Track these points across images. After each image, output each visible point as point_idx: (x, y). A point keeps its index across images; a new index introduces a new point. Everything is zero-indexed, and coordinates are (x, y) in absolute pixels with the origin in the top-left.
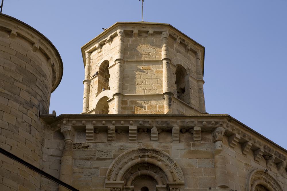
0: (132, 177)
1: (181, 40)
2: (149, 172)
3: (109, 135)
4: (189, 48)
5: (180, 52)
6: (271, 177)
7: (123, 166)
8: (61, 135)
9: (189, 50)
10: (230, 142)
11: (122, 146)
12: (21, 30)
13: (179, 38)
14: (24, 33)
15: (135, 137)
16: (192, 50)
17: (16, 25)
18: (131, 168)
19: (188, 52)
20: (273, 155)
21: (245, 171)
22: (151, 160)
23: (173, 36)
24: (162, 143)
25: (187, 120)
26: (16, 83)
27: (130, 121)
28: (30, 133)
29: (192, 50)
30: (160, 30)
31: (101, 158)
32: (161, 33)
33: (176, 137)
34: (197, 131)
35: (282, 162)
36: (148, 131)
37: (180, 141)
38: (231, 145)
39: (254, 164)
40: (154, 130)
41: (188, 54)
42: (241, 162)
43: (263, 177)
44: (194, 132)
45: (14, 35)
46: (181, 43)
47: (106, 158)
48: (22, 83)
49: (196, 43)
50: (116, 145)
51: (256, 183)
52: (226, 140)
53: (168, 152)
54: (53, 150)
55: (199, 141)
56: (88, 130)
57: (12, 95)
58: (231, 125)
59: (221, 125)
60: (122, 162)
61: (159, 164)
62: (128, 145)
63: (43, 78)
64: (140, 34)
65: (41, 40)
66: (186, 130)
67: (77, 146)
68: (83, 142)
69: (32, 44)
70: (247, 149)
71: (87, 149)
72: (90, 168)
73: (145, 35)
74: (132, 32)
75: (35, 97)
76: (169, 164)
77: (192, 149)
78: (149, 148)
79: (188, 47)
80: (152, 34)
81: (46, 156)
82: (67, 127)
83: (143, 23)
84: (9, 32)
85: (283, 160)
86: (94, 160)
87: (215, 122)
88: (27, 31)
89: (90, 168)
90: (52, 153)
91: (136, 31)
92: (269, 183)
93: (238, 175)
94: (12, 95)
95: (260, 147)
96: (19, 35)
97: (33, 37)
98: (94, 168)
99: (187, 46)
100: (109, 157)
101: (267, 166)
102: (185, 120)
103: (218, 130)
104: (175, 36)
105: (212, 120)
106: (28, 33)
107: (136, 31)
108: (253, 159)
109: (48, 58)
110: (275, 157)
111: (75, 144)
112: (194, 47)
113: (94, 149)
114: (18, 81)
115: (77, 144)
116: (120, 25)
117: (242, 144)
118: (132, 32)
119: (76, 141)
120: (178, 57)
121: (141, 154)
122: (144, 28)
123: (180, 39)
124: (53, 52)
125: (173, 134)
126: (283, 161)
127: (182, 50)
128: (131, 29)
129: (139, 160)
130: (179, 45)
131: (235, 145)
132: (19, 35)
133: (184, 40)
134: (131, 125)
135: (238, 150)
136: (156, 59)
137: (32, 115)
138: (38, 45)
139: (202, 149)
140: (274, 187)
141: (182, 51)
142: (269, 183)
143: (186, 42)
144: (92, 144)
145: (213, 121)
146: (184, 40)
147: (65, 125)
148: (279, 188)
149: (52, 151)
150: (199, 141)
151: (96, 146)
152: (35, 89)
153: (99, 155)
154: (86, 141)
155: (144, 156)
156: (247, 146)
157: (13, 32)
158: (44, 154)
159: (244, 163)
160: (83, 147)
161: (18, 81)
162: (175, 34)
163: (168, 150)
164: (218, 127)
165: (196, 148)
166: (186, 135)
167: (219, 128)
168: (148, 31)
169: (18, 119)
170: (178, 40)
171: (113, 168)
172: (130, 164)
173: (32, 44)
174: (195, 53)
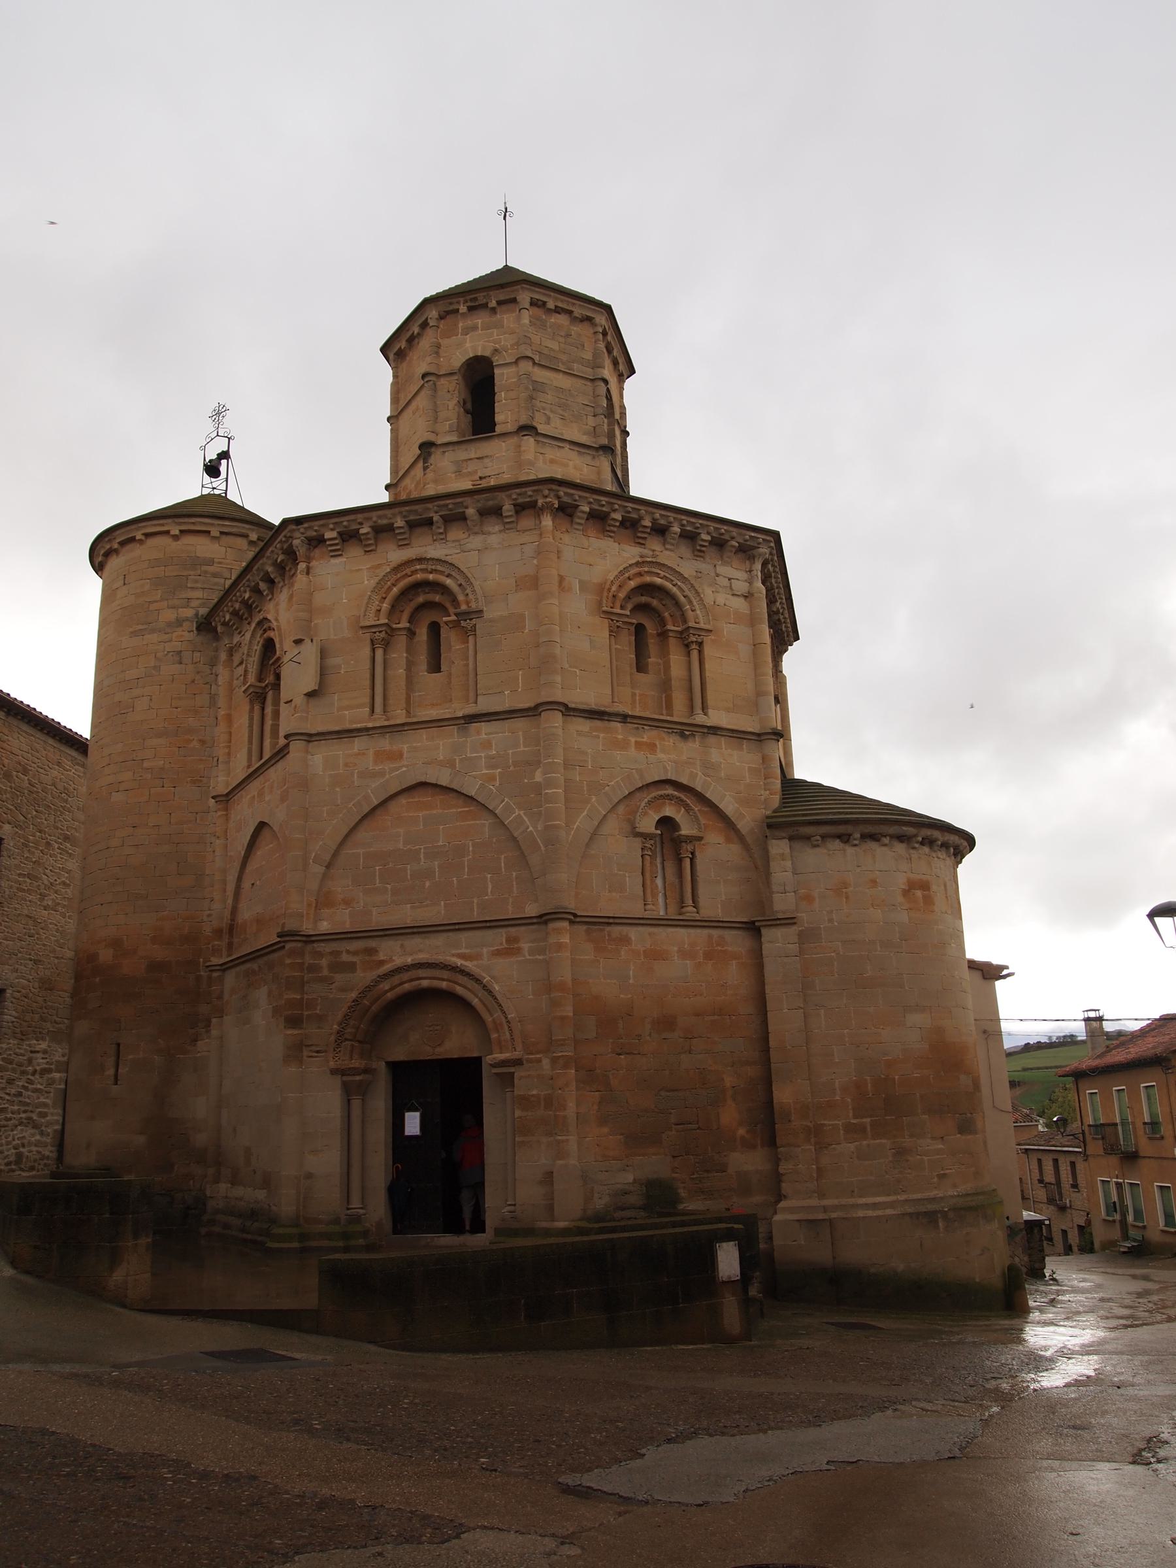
5: (475, 328)
12: (144, 527)
13: (464, 303)
21: (366, 582)
26: (153, 607)
27: (240, 589)
35: (464, 512)
40: (263, 586)
41: (498, 316)
42: (359, 570)
48: (162, 600)
58: (305, 528)
63: (205, 568)
75: (187, 606)
84: (132, 540)
93: (344, 601)
96: (147, 535)
99: (487, 303)
106: (155, 525)
118: (401, 347)
119: (235, 642)
120: (468, 345)
121: (261, 632)
123: (467, 302)
127: (480, 319)
128: (399, 347)
132: (147, 535)
146: (475, 299)
148: (456, 570)
152: (184, 596)
155: (265, 631)
157: (137, 538)
159: (367, 568)
169: (158, 655)
173: (167, 532)
174: (514, 301)
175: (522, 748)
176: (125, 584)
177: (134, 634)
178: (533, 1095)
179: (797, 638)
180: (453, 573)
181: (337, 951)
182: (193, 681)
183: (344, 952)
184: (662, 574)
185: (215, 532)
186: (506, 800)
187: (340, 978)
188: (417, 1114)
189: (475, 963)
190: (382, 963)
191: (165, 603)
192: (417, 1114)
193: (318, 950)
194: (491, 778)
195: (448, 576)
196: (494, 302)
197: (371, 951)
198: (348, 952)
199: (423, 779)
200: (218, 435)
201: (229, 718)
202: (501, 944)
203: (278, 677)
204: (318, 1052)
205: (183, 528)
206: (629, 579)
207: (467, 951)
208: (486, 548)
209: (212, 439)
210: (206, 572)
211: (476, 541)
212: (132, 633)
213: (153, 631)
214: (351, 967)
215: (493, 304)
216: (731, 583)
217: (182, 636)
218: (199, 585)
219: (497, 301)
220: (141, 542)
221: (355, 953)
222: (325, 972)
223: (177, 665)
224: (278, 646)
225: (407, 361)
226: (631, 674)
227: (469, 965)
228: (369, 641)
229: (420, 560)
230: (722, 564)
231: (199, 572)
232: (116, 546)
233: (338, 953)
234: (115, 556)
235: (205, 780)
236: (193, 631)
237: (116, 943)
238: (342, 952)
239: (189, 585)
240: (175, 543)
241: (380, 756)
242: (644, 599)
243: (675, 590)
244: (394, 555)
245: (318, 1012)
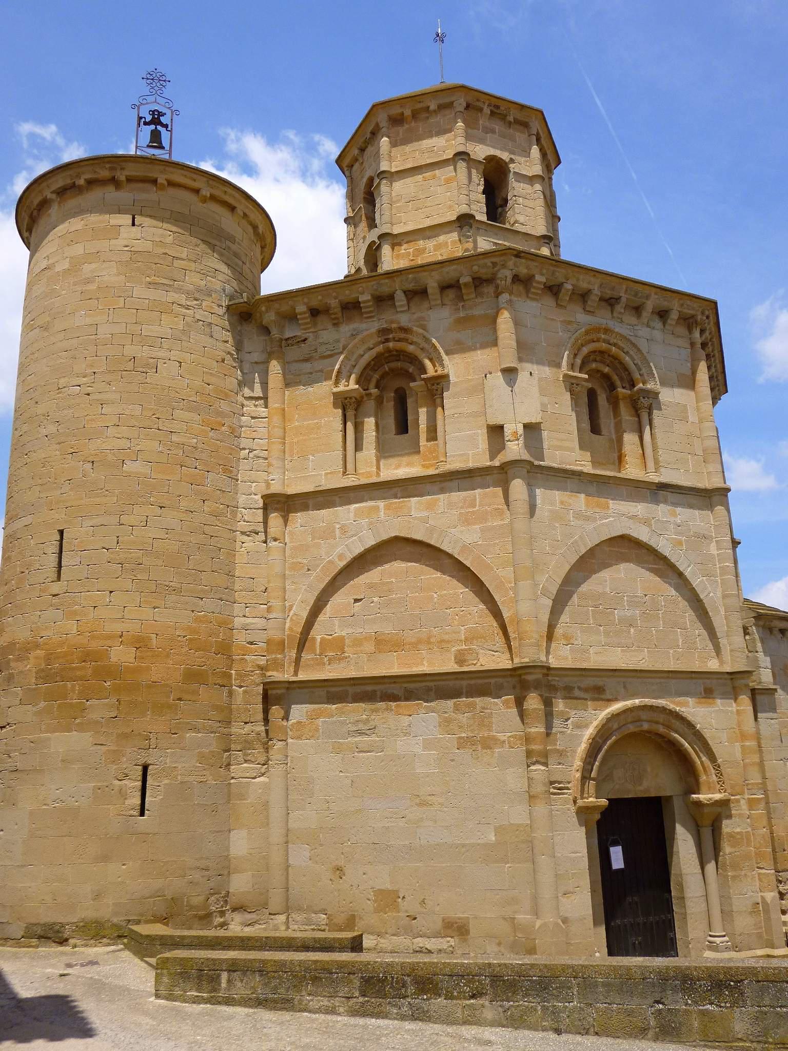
0: (376, 376)
1: (492, 108)
2: (399, 364)
3: (333, 316)
4: (511, 119)
5: (493, 131)
6: (617, 333)
7: (357, 361)
8: (266, 330)
9: (510, 123)
10: (528, 291)
11: (354, 330)
14: (178, 177)
15: (371, 312)
16: (517, 122)
17: (162, 168)
18: (373, 363)
19: (510, 127)
20: (622, 294)
21: (561, 334)
22: (399, 345)
23: (475, 104)
24: (414, 314)
25: (446, 270)
26: (177, 263)
29: (517, 122)
30: (447, 100)
31: (325, 354)
32: (450, 105)
33: (436, 300)
34: (466, 284)
35: (644, 303)
36: (391, 297)
37: (443, 305)
38: (530, 295)
39: (582, 318)
42: (553, 320)
43: (603, 336)
44: (462, 287)
45: (162, 184)
46: (492, 113)
47: (333, 352)
49: (523, 107)
50: (346, 329)
51: (585, 350)
52: (521, 288)
53: (424, 328)
54: (258, 353)
55: (473, 299)
56: (300, 314)
57: (171, 283)
59: (504, 266)
60: (355, 356)
61: (411, 348)
62: (364, 326)
63: (227, 242)
64: (415, 115)
65: (211, 182)
66: (450, 286)
67: (290, 342)
68: (299, 334)
69: (197, 191)
70: (564, 296)
71: (305, 343)
72: (311, 373)
73: (425, 115)
74: (403, 114)
76: (426, 346)
77: (462, 315)
78: (394, 326)
79: (508, 117)
80: (435, 111)
81: (248, 366)
82: (269, 317)
83: (443, 86)
84: (154, 182)
85: (644, 301)
86: (316, 359)
87: (492, 263)
88: (182, 172)
89: (311, 373)
90: (256, 360)
91: (408, 112)
92: (615, 345)
94: (171, 283)
95: (591, 287)
96: (171, 184)
97: (195, 180)
98: (316, 372)
99: (506, 116)
100: (336, 351)
101: (613, 317)
102: (444, 269)
103: (500, 275)
104: (480, 104)
105: (486, 261)
107: (408, 112)
108: (581, 310)
109: (233, 209)
110: (627, 298)
111: (287, 340)
112: (520, 116)
113: (314, 343)
114: (178, 258)
115: (288, 338)
116: (380, 106)
117: (553, 290)
119: (288, 334)
121: (382, 339)
122: (420, 102)
124: (237, 195)
125: (430, 297)
126: (645, 303)
127: (498, 126)
128: (399, 111)
129: (380, 348)
130: (489, 119)
131: (536, 294)
132: (171, 184)
133: (497, 106)
134: (362, 293)
135: (549, 301)
136: (445, 157)
137: (211, 307)
138: (206, 192)
139: (478, 311)
140: (625, 350)
141: (497, 127)
142: (615, 345)
143: (504, 109)
144: (311, 334)
145: (488, 262)
146: (498, 107)
147: (267, 311)
149: (256, 357)
150: (473, 299)
151: (316, 337)
152: (212, 265)
153: (322, 349)
154: (303, 332)
155: (387, 340)
156: (563, 291)
157: (159, 181)
158: (244, 363)
160: (298, 342)
161: (178, 258)
162: (478, 100)
163: (425, 323)
164: (499, 270)
165: (467, 312)
166: (451, 294)
167: (502, 271)
168: (429, 107)
170: (487, 111)
171: (343, 367)
172: (368, 357)
173: (197, 191)
174: (525, 125)
176: (133, 224)
178: (738, 833)
180: (631, 353)
181: (571, 687)
183: (576, 689)
185: (239, 211)
188: (619, 848)
192: (619, 848)
193: (552, 683)
195: (627, 353)
196: (512, 117)
198: (579, 688)
200: (156, 102)
204: (560, 789)
205: (217, 193)
208: (652, 340)
209: (147, 103)
210: (229, 248)
211: (644, 332)
213: (179, 290)
215: (511, 119)
219: (514, 118)
220: (162, 188)
225: (404, 128)
229: (607, 331)
232: (123, 178)
234: (111, 188)
235: (235, 473)
236: (222, 306)
237: (140, 643)
238: (574, 687)
240: (201, 204)
244: (603, 318)
245: (558, 747)
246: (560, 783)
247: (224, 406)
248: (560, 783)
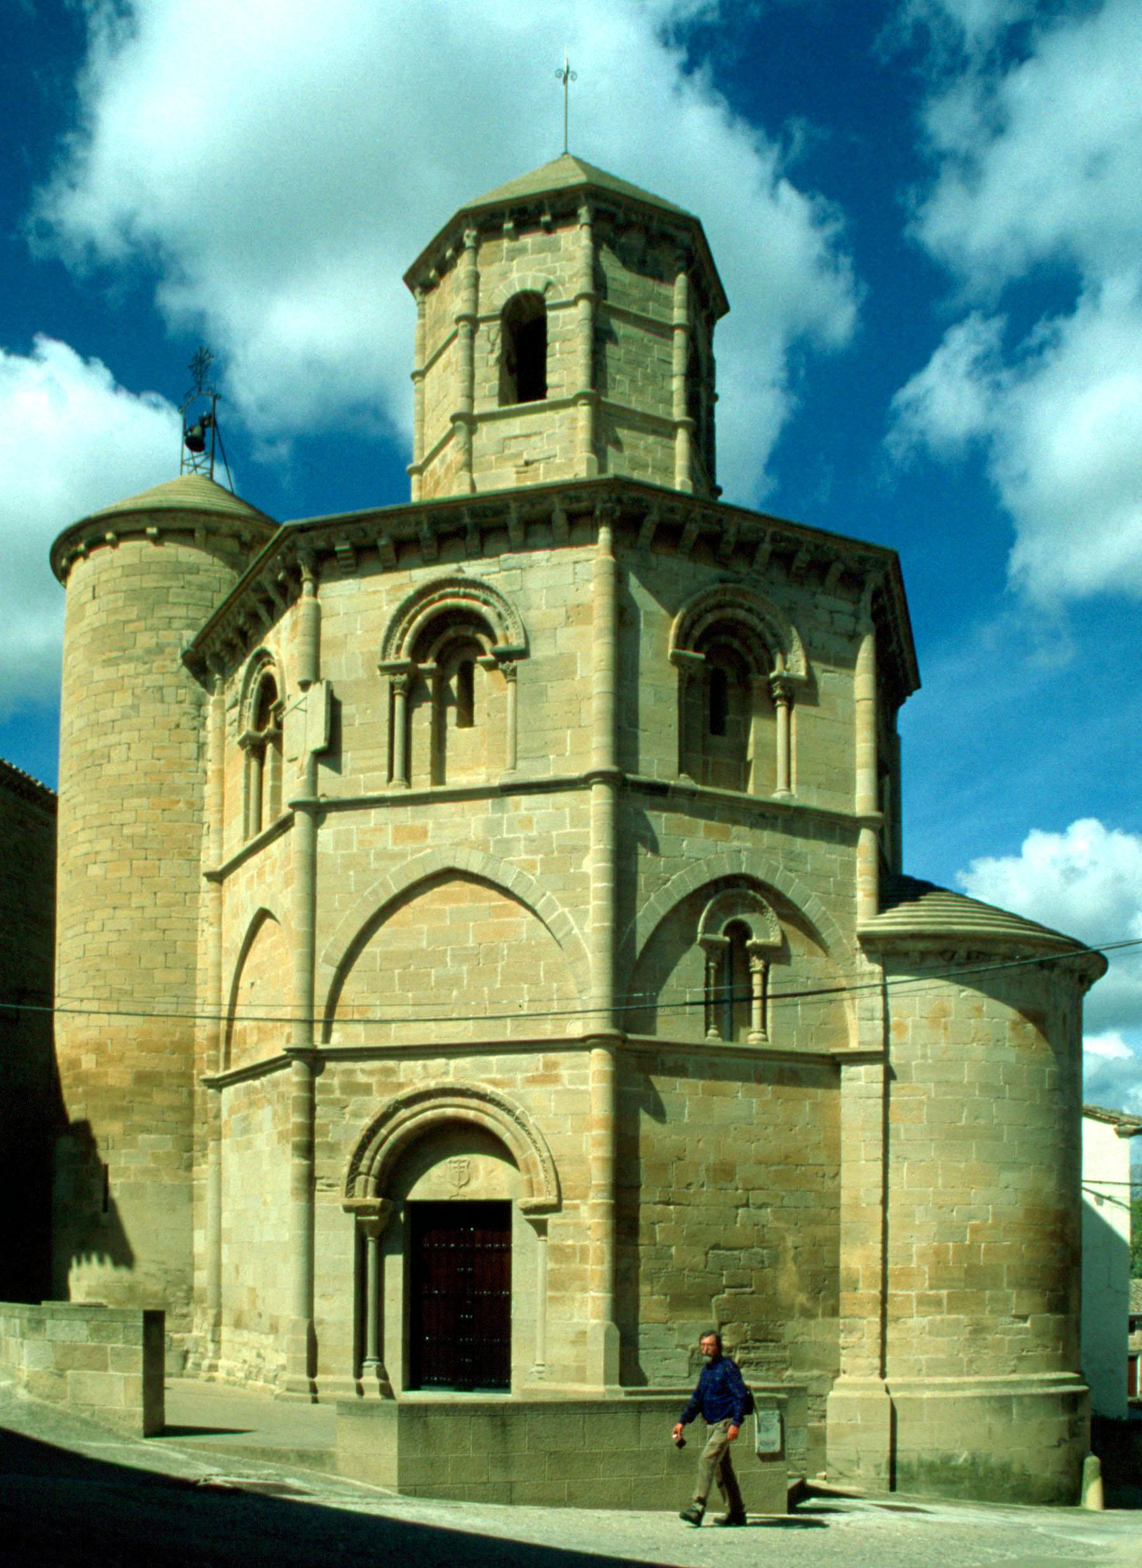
26: (130, 627)
28: (162, 701)
48: (139, 619)
63: (189, 577)
175: (568, 830)
176: (94, 598)
177: (108, 663)
179: (918, 686)
182: (178, 726)
184: (747, 604)
186: (548, 893)
187: (355, 1102)
189: (507, 1090)
190: (400, 1086)
191: (142, 624)
194: (532, 865)
197: (389, 1072)
198: (363, 1071)
199: (449, 863)
201: (221, 774)
202: (537, 1069)
203: (279, 725)
204: (330, 1185)
206: (707, 611)
207: (499, 1077)
210: (189, 583)
212: (104, 661)
213: (130, 659)
214: (367, 1089)
216: (832, 618)
217: (163, 667)
218: (182, 600)
221: (371, 1073)
222: (337, 1094)
223: (159, 705)
224: (279, 687)
226: (704, 736)
227: (500, 1092)
228: (387, 687)
230: (823, 593)
231: (182, 583)
233: (352, 1072)
234: (81, 560)
235: (194, 852)
239: (171, 599)
241: (402, 833)
242: (723, 639)
243: (760, 627)
246: (329, 1178)
247: (179, 779)
248: (329, 1178)
